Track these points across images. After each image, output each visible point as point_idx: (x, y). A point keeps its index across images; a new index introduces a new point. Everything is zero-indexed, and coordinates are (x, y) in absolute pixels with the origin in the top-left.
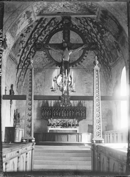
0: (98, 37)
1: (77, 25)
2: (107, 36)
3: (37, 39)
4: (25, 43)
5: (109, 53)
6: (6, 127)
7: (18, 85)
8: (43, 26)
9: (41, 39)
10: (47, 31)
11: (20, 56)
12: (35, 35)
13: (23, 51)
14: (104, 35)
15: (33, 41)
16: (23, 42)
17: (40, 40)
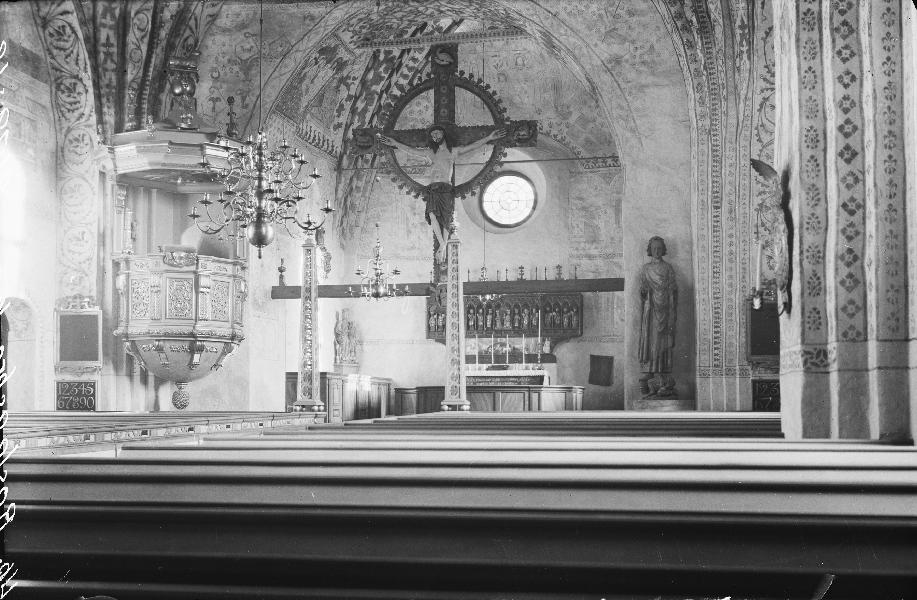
3: (400, 64)
4: (357, 82)
6: (288, 374)
7: (345, 224)
11: (344, 126)
13: (353, 111)
15: (386, 70)
16: (349, 81)
17: (411, 64)
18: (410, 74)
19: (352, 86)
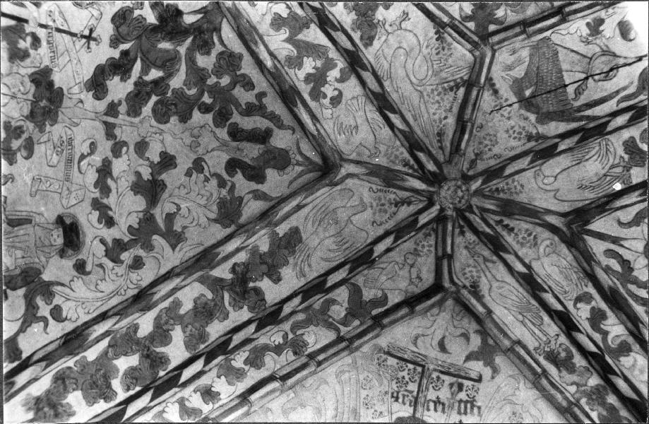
1: (531, 343)
4: (57, 330)
8: (258, 291)
10: (278, 350)
12: (161, 334)
19: (37, 328)
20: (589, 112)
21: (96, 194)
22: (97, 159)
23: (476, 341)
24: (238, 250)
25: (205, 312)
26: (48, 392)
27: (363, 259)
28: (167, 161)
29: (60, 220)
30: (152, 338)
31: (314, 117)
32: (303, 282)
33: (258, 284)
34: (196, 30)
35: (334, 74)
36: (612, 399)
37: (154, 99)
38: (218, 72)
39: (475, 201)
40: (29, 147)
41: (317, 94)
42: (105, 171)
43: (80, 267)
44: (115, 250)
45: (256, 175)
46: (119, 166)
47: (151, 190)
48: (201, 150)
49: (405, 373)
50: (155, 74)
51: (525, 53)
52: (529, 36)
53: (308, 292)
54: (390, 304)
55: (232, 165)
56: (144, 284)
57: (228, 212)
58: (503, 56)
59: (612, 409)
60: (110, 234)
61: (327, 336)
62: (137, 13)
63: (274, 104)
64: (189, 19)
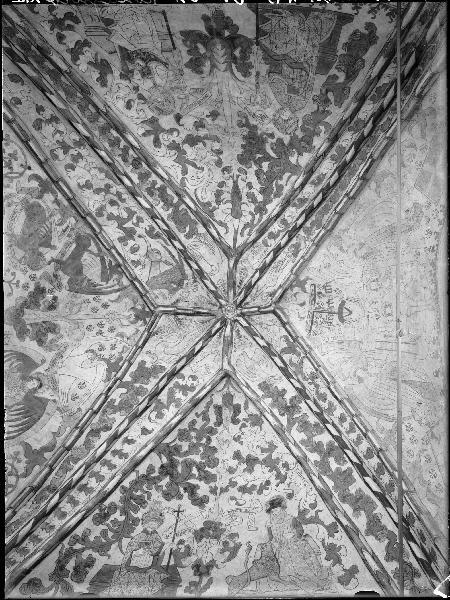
0: (305, 159)
1: (291, 265)
2: (276, 123)
4: (321, 505)
5: (333, 71)
8: (291, 400)
9: (342, 419)
10: (317, 386)
12: (317, 448)
13: (352, 533)
14: (287, 140)
18: (358, 432)
20: (177, 257)
21: (255, 492)
22: (238, 495)
23: (296, 289)
24: (273, 415)
25: (305, 426)
26: (351, 505)
27: (268, 349)
28: (237, 455)
29: (268, 511)
30: (320, 452)
31: (204, 388)
32: (284, 378)
33: (288, 402)
34: (170, 455)
35: (181, 382)
36: (308, 224)
37: (207, 469)
38: (188, 438)
39: (231, 301)
40: (233, 536)
41: (192, 388)
42: (243, 489)
43: (290, 496)
44: (281, 478)
45: (237, 410)
46: (241, 482)
47: (251, 461)
48: (230, 439)
49: (318, 321)
50: (195, 471)
51: (156, 292)
52: (147, 292)
53: (288, 376)
54: (286, 334)
55: (235, 421)
56: (295, 460)
57: (256, 421)
58: (160, 301)
59: (312, 224)
60: (274, 481)
61: (306, 362)
62: (164, 488)
63: (201, 408)
64: (165, 460)
